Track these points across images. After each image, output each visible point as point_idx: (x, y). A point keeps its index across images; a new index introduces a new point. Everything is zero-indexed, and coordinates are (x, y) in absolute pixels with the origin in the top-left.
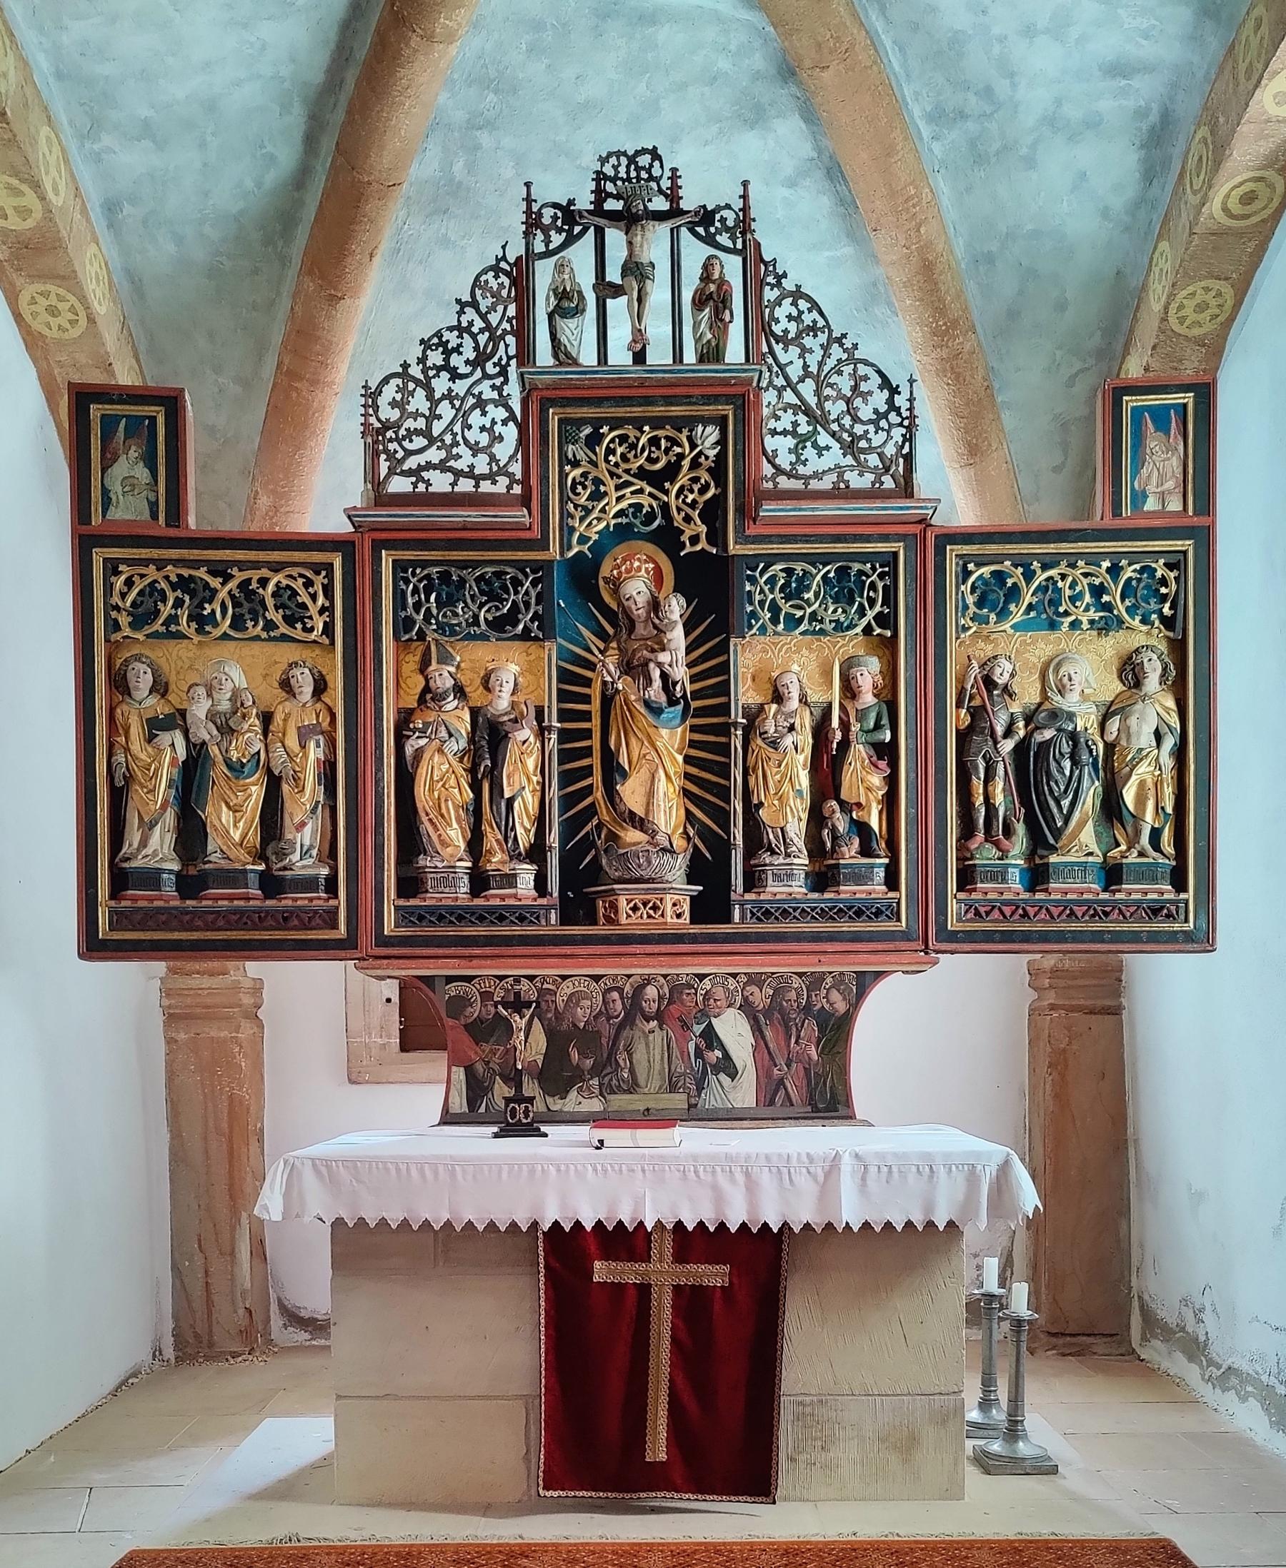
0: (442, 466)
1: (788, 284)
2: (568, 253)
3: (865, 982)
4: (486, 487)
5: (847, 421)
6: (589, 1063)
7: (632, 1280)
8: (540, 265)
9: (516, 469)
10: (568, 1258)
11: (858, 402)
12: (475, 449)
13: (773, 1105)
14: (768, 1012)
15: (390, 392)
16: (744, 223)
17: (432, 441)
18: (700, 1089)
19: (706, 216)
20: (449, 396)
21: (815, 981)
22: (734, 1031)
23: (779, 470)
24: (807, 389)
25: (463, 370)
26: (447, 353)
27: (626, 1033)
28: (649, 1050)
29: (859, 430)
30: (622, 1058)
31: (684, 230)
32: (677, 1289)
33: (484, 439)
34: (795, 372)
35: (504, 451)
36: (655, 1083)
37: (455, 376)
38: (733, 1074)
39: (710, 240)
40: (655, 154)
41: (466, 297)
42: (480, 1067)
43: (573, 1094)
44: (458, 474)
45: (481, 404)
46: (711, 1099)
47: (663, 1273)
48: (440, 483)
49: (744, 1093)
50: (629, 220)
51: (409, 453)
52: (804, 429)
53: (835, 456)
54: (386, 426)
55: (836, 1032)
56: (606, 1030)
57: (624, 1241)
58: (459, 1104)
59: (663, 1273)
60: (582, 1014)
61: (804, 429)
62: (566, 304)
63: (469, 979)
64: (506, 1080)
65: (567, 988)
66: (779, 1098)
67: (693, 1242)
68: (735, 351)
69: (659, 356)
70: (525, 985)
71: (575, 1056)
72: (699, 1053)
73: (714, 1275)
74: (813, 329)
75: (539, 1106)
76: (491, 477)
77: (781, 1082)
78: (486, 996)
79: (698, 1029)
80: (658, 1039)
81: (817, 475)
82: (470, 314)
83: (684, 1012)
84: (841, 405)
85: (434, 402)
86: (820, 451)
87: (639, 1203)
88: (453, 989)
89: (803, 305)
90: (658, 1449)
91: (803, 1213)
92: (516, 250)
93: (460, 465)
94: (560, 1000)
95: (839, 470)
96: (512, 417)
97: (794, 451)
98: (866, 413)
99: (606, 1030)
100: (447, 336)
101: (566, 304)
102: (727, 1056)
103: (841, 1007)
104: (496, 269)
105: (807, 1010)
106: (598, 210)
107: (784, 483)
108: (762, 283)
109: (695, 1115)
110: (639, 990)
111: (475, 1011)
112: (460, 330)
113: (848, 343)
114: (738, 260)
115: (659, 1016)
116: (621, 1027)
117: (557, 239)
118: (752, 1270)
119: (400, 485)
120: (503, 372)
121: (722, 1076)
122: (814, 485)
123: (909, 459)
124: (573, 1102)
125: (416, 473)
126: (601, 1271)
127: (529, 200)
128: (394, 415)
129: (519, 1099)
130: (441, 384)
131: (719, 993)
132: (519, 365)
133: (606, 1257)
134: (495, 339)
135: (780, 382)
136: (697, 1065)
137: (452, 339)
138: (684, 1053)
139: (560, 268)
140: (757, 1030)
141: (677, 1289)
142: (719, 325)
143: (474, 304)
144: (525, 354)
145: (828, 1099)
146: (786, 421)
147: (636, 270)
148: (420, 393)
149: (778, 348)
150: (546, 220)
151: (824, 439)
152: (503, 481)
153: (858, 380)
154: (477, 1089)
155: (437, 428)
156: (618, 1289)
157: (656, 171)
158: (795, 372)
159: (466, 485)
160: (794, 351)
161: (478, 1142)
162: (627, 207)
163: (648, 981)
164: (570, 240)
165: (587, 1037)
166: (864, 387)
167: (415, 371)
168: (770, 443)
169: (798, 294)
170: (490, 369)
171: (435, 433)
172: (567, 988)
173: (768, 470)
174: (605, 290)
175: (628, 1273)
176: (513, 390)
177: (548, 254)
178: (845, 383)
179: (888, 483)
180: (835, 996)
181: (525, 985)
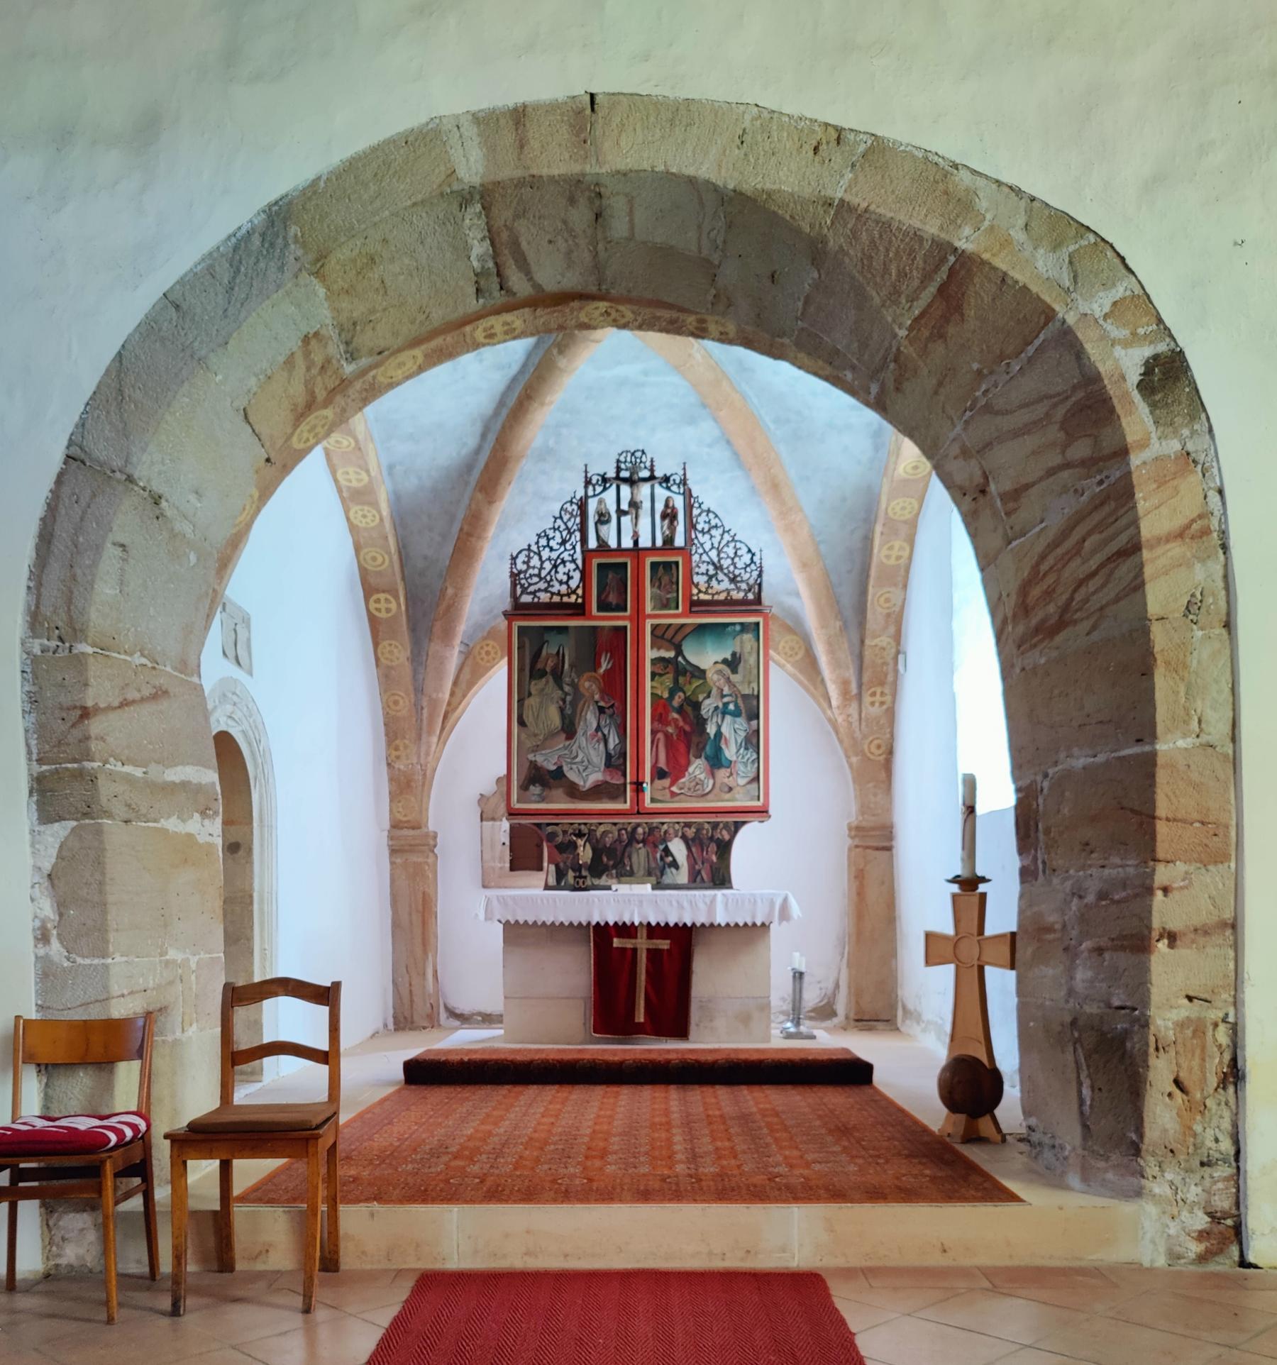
0: (546, 590)
1: (704, 507)
2: (602, 496)
3: (738, 826)
4: (565, 599)
5: (732, 568)
6: (611, 863)
7: (629, 946)
8: (590, 501)
9: (580, 592)
11: (737, 560)
12: (561, 583)
13: (696, 881)
14: (693, 840)
15: (522, 557)
16: (684, 482)
17: (541, 579)
18: (662, 875)
19: (666, 479)
20: (549, 559)
21: (715, 826)
22: (678, 849)
23: (700, 591)
24: (713, 554)
25: (556, 547)
26: (548, 540)
27: (628, 849)
28: (639, 856)
29: (737, 572)
30: (626, 861)
31: (657, 486)
32: (648, 950)
33: (565, 579)
34: (707, 547)
35: (574, 583)
36: (642, 872)
37: (552, 549)
38: (677, 867)
39: (668, 488)
40: (643, 452)
41: (557, 515)
42: (562, 865)
43: (604, 877)
44: (553, 594)
45: (563, 562)
46: (667, 879)
48: (544, 597)
49: (683, 876)
50: (631, 482)
51: (530, 584)
52: (712, 572)
53: (726, 584)
54: (520, 572)
55: (724, 849)
56: (620, 848)
57: (626, 930)
58: (552, 881)
60: (608, 840)
61: (712, 572)
62: (603, 518)
63: (557, 824)
64: (574, 870)
65: (602, 829)
66: (699, 879)
67: (655, 931)
68: (679, 541)
69: (645, 542)
70: (583, 827)
71: (605, 859)
72: (662, 859)
73: (664, 944)
74: (716, 527)
75: (588, 882)
76: (568, 595)
77: (699, 872)
78: (565, 832)
79: (662, 847)
80: (643, 852)
81: (717, 593)
82: (559, 522)
84: (729, 561)
85: (542, 562)
86: (719, 582)
87: (632, 914)
88: (550, 829)
89: (711, 516)
90: (640, 1017)
91: (701, 919)
92: (580, 493)
93: (554, 590)
94: (598, 834)
95: (728, 591)
96: (578, 567)
97: (708, 582)
98: (740, 564)
99: (620, 848)
100: (548, 532)
101: (603, 518)
102: (674, 860)
103: (727, 837)
104: (571, 502)
105: (711, 838)
106: (618, 478)
107: (702, 596)
108: (692, 507)
110: (634, 829)
111: (560, 839)
112: (554, 529)
113: (732, 533)
114: (681, 498)
115: (644, 841)
116: (626, 846)
117: (599, 489)
118: (681, 942)
119: (526, 599)
120: (574, 548)
121: (673, 870)
122: (716, 597)
123: (760, 585)
125: (534, 593)
126: (616, 942)
127: (586, 472)
128: (524, 567)
129: (581, 877)
130: (546, 554)
131: (671, 831)
132: (582, 546)
133: (619, 936)
134: (570, 533)
135: (700, 551)
136: (661, 864)
137: (551, 534)
138: (655, 858)
139: (600, 502)
140: (689, 848)
141: (648, 950)
142: (672, 528)
143: (561, 517)
144: (584, 540)
145: (721, 879)
146: (703, 568)
147: (634, 505)
148: (536, 558)
149: (700, 536)
150: (594, 481)
151: (721, 576)
152: (573, 598)
153: (736, 550)
154: (560, 875)
155: (543, 573)
156: (623, 950)
157: (644, 459)
158: (707, 547)
159: (556, 599)
160: (707, 536)
162: (632, 474)
163: (638, 825)
164: (605, 489)
165: (610, 851)
166: (739, 553)
167: (534, 548)
168: (696, 579)
169: (709, 511)
170: (568, 546)
171: (543, 575)
172: (602, 829)
173: (695, 591)
174: (621, 513)
175: (628, 944)
176: (578, 556)
177: (595, 495)
178: (731, 551)
179: (751, 596)
180: (724, 832)
181: (583, 827)
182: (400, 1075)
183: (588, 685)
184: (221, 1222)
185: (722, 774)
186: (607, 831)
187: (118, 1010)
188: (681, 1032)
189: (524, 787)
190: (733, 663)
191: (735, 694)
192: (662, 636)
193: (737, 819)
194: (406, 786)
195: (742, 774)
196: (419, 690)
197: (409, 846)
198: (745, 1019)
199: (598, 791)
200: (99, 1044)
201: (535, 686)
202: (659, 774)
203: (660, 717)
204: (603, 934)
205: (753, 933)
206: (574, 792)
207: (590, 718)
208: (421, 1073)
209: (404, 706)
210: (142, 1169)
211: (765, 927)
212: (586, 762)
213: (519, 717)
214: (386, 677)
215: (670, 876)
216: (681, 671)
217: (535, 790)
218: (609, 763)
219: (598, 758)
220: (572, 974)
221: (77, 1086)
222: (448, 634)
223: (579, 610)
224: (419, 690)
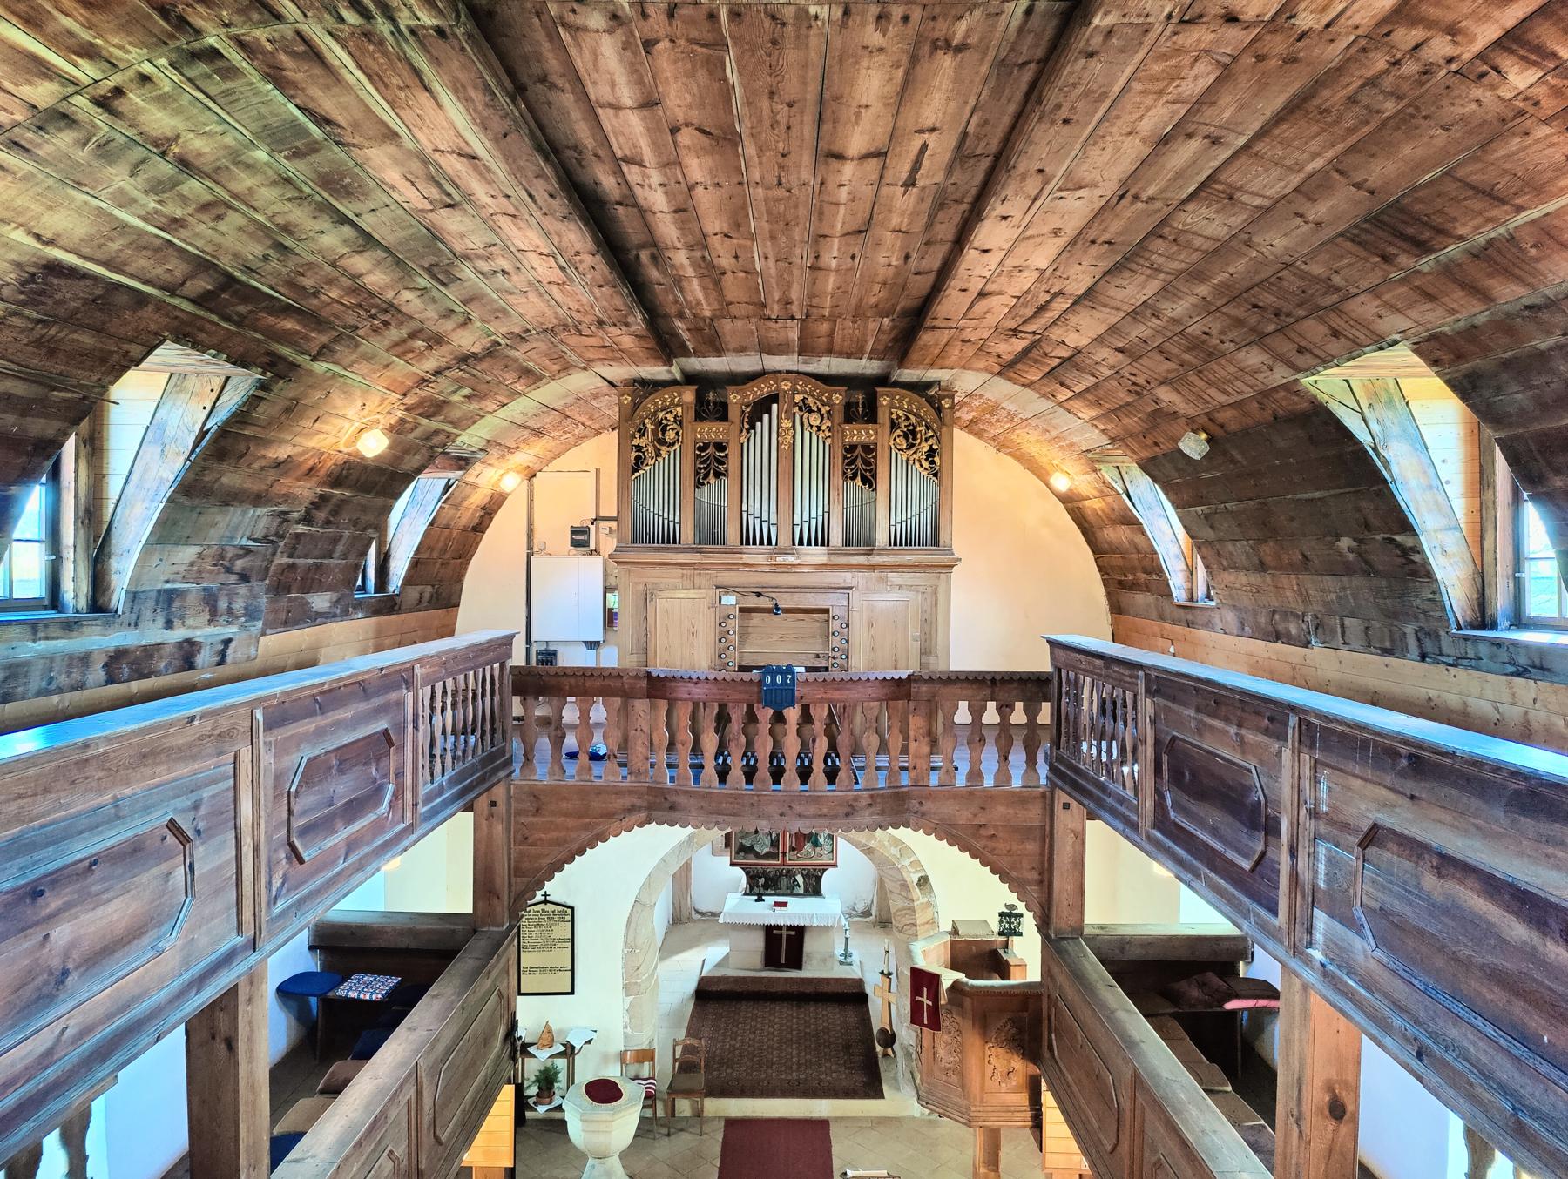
22: (800, 879)
28: (784, 882)
47: (784, 932)
55: (819, 879)
57: (779, 927)
59: (784, 932)
67: (790, 928)
91: (807, 923)
154: (751, 888)
182: (692, 986)
187: (645, 1046)
188: (799, 967)
193: (823, 868)
195: (827, 849)
198: (824, 960)
199: (768, 856)
202: (793, 849)
204: (769, 929)
206: (758, 856)
220: (758, 942)
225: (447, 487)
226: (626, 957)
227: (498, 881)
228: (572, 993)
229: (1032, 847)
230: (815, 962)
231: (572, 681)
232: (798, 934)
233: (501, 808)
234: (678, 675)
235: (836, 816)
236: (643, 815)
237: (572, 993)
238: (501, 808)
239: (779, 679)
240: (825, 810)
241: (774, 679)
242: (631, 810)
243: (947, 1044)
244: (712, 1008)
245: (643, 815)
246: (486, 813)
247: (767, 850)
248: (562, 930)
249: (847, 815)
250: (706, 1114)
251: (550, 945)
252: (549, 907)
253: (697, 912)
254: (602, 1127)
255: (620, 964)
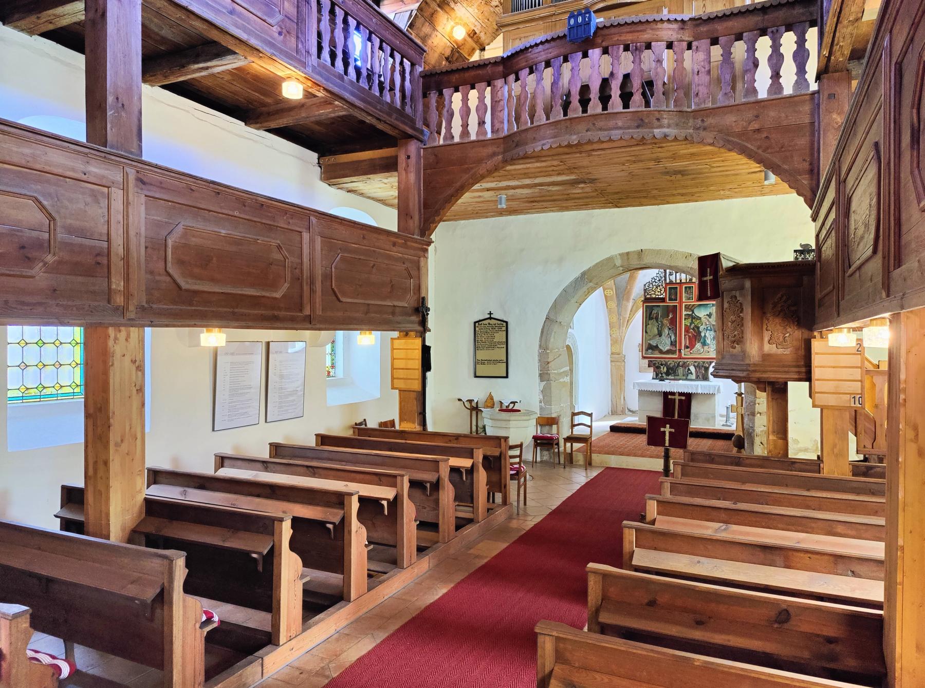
10: (666, 394)
13: (697, 378)
22: (692, 369)
28: (680, 371)
47: (677, 397)
49: (694, 377)
57: (673, 394)
59: (677, 397)
67: (681, 394)
73: (683, 398)
83: (685, 366)
109: (686, 379)
124: (670, 377)
154: (657, 375)
161: (657, 381)
165: (672, 369)
183: (666, 322)
184: (571, 454)
185: (706, 347)
186: (671, 363)
187: (553, 416)
189: (647, 350)
190: (710, 315)
191: (710, 324)
192: (687, 308)
194: (616, 341)
196: (619, 314)
197: (617, 359)
199: (668, 352)
200: (551, 422)
201: (650, 322)
203: (687, 331)
205: (710, 396)
206: (661, 352)
207: (666, 331)
208: (614, 429)
209: (615, 319)
210: (558, 444)
211: (713, 395)
212: (665, 343)
213: (645, 331)
214: (610, 311)
215: (690, 377)
216: (693, 318)
217: (650, 351)
218: (671, 344)
219: (668, 342)
221: (546, 429)
222: (628, 300)
223: (663, 300)
224: (619, 314)
225: (411, 15)
226: (540, 355)
227: (411, 204)
228: (507, 377)
229: (803, 141)
230: (700, 420)
231: (457, 76)
232: (688, 399)
233: (413, 160)
234: (518, 50)
235: (629, 128)
236: (500, 157)
237: (507, 377)
238: (413, 160)
239: (580, 19)
240: (620, 124)
241: (576, 21)
242: (494, 154)
243: (733, 322)
244: (617, 435)
245: (500, 157)
246: (404, 165)
247: (668, 348)
248: (500, 336)
249: (638, 127)
250: (593, 464)
251: (493, 346)
252: (492, 322)
253: (630, 411)
254: (503, 424)
255: (537, 358)
